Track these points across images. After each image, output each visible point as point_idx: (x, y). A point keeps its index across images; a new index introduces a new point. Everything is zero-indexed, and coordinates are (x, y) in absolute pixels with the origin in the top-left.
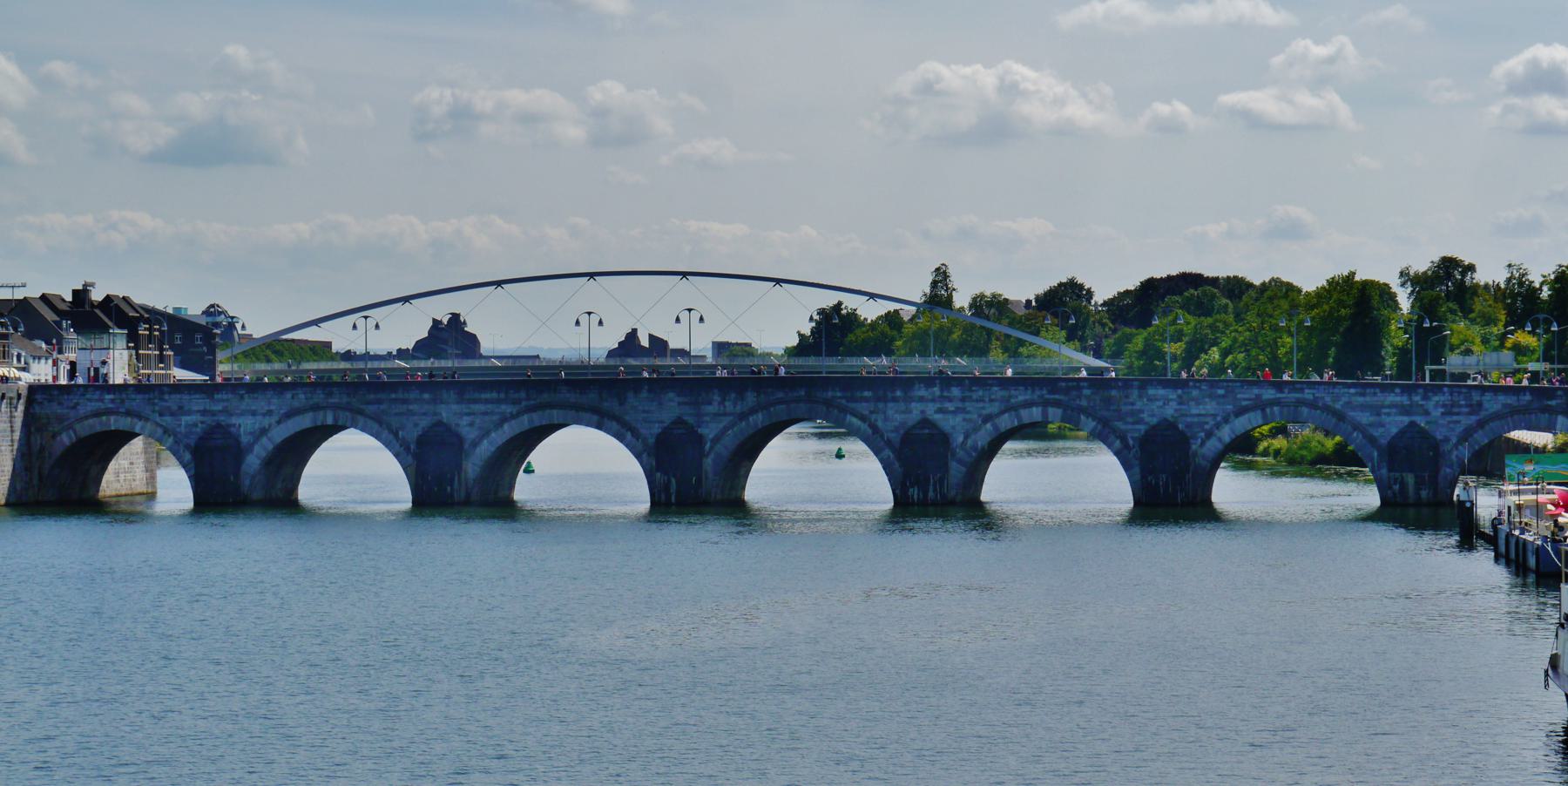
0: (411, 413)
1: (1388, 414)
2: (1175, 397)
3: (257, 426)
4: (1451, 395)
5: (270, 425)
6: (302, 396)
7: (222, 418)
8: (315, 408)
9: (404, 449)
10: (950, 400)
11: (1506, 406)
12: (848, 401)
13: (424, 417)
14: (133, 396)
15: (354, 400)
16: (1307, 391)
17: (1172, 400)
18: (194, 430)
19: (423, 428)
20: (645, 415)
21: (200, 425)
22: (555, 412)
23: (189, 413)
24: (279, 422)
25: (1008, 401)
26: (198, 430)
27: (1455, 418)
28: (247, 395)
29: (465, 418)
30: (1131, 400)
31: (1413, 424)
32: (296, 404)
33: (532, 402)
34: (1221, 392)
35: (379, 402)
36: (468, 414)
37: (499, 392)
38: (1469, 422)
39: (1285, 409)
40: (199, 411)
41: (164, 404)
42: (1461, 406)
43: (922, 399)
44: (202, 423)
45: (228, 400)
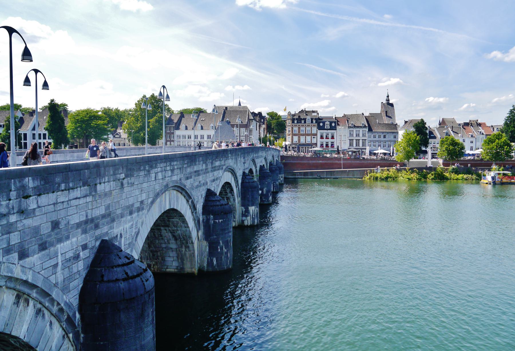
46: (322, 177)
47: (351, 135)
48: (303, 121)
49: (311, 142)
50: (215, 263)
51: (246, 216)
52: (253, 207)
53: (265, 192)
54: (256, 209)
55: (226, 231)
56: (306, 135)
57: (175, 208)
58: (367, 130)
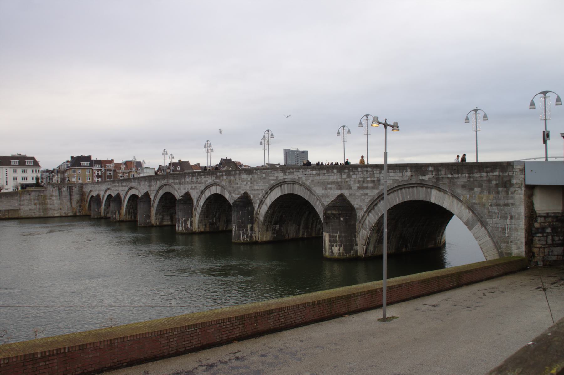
1: (330, 188)
2: (249, 179)
4: (363, 173)
11: (395, 181)
12: (174, 184)
16: (295, 173)
17: (248, 181)
25: (206, 183)
27: (365, 191)
30: (237, 182)
31: (341, 196)
34: (264, 175)
38: (373, 195)
39: (289, 185)
42: (368, 182)
43: (188, 183)
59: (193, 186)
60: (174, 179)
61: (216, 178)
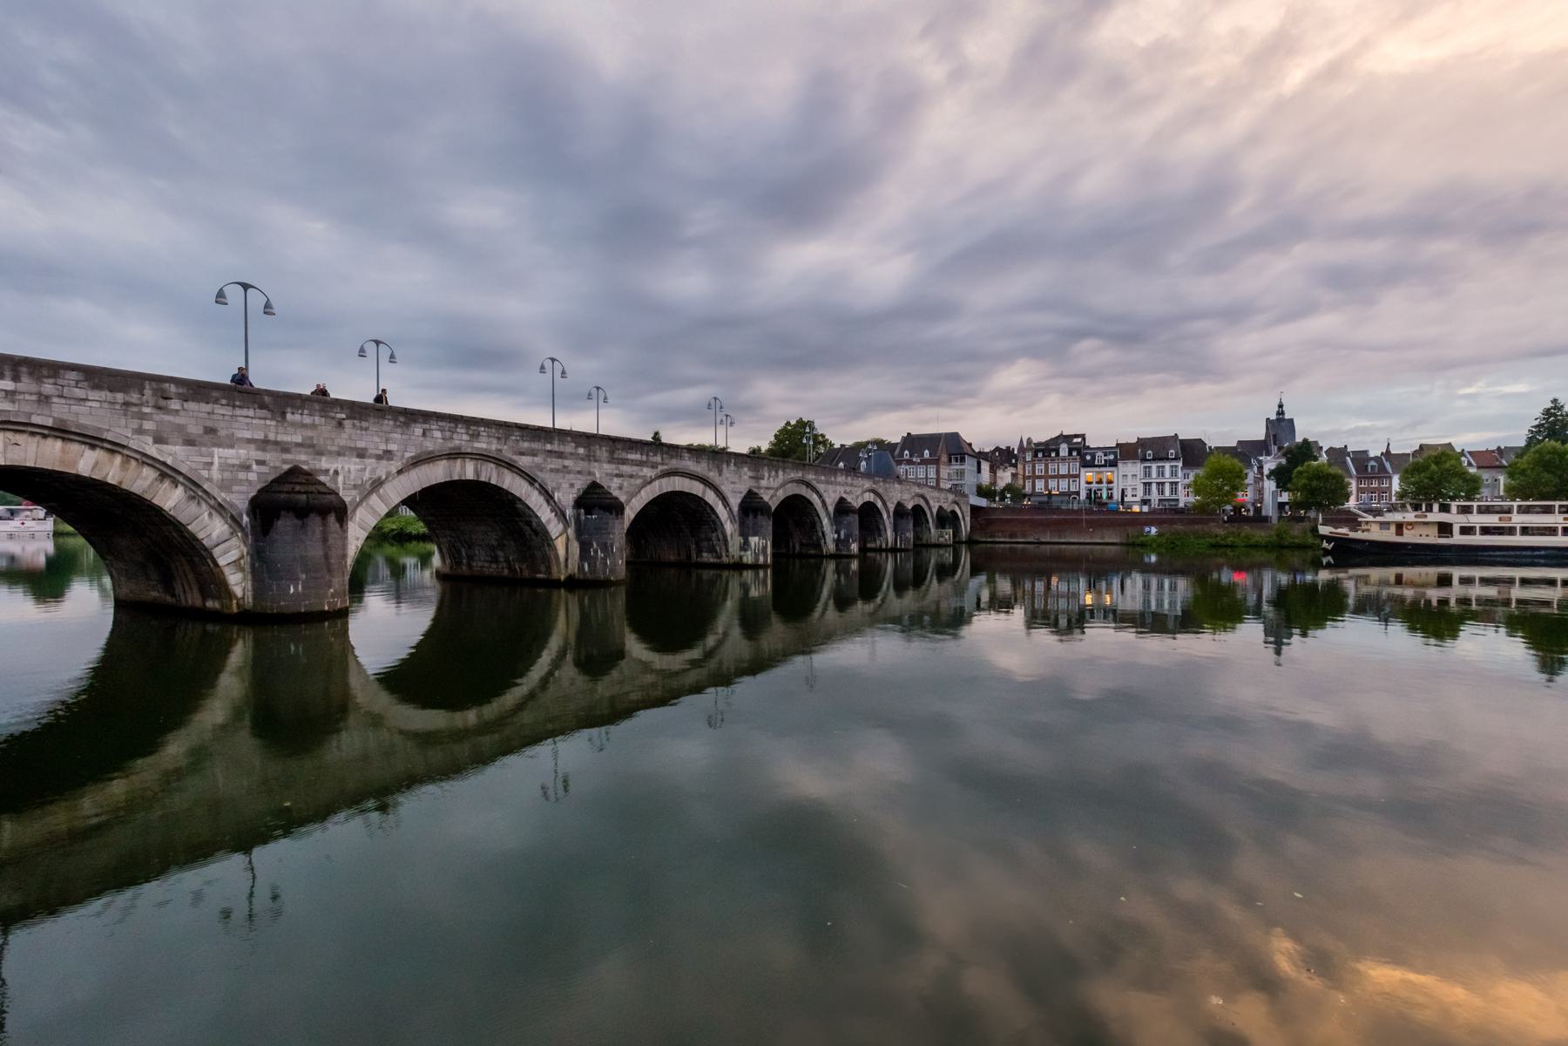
0: (566, 470)
3: (367, 476)
5: (388, 474)
6: (438, 434)
7: (303, 457)
8: (455, 455)
9: (556, 515)
10: (847, 484)
13: (579, 476)
14: (79, 393)
15: (505, 447)
18: (242, 475)
19: (579, 490)
20: (732, 486)
21: (254, 467)
22: (677, 478)
23: (231, 443)
24: (400, 472)
26: (252, 476)
28: (348, 423)
29: (615, 480)
32: (429, 445)
33: (666, 467)
35: (533, 453)
36: (618, 476)
37: (641, 454)
40: (250, 441)
41: (167, 418)
43: (839, 484)
44: (260, 463)
45: (314, 426)
46: (1043, 540)
47: (1147, 473)
48: (1053, 455)
49: (1069, 489)
50: (587, 569)
51: (746, 550)
52: (756, 539)
53: (842, 537)
54: (761, 541)
55: (603, 531)
56: (1046, 477)
57: (493, 482)
58: (1180, 464)
59: (848, 489)
60: (815, 475)
61: (874, 483)
